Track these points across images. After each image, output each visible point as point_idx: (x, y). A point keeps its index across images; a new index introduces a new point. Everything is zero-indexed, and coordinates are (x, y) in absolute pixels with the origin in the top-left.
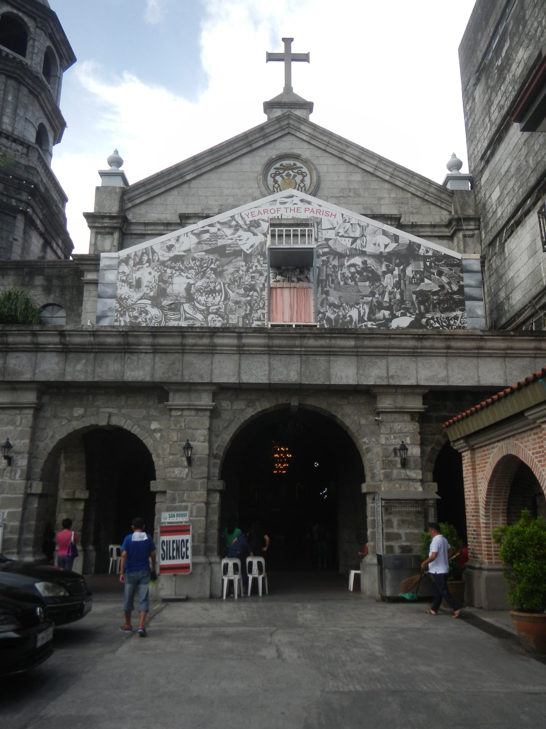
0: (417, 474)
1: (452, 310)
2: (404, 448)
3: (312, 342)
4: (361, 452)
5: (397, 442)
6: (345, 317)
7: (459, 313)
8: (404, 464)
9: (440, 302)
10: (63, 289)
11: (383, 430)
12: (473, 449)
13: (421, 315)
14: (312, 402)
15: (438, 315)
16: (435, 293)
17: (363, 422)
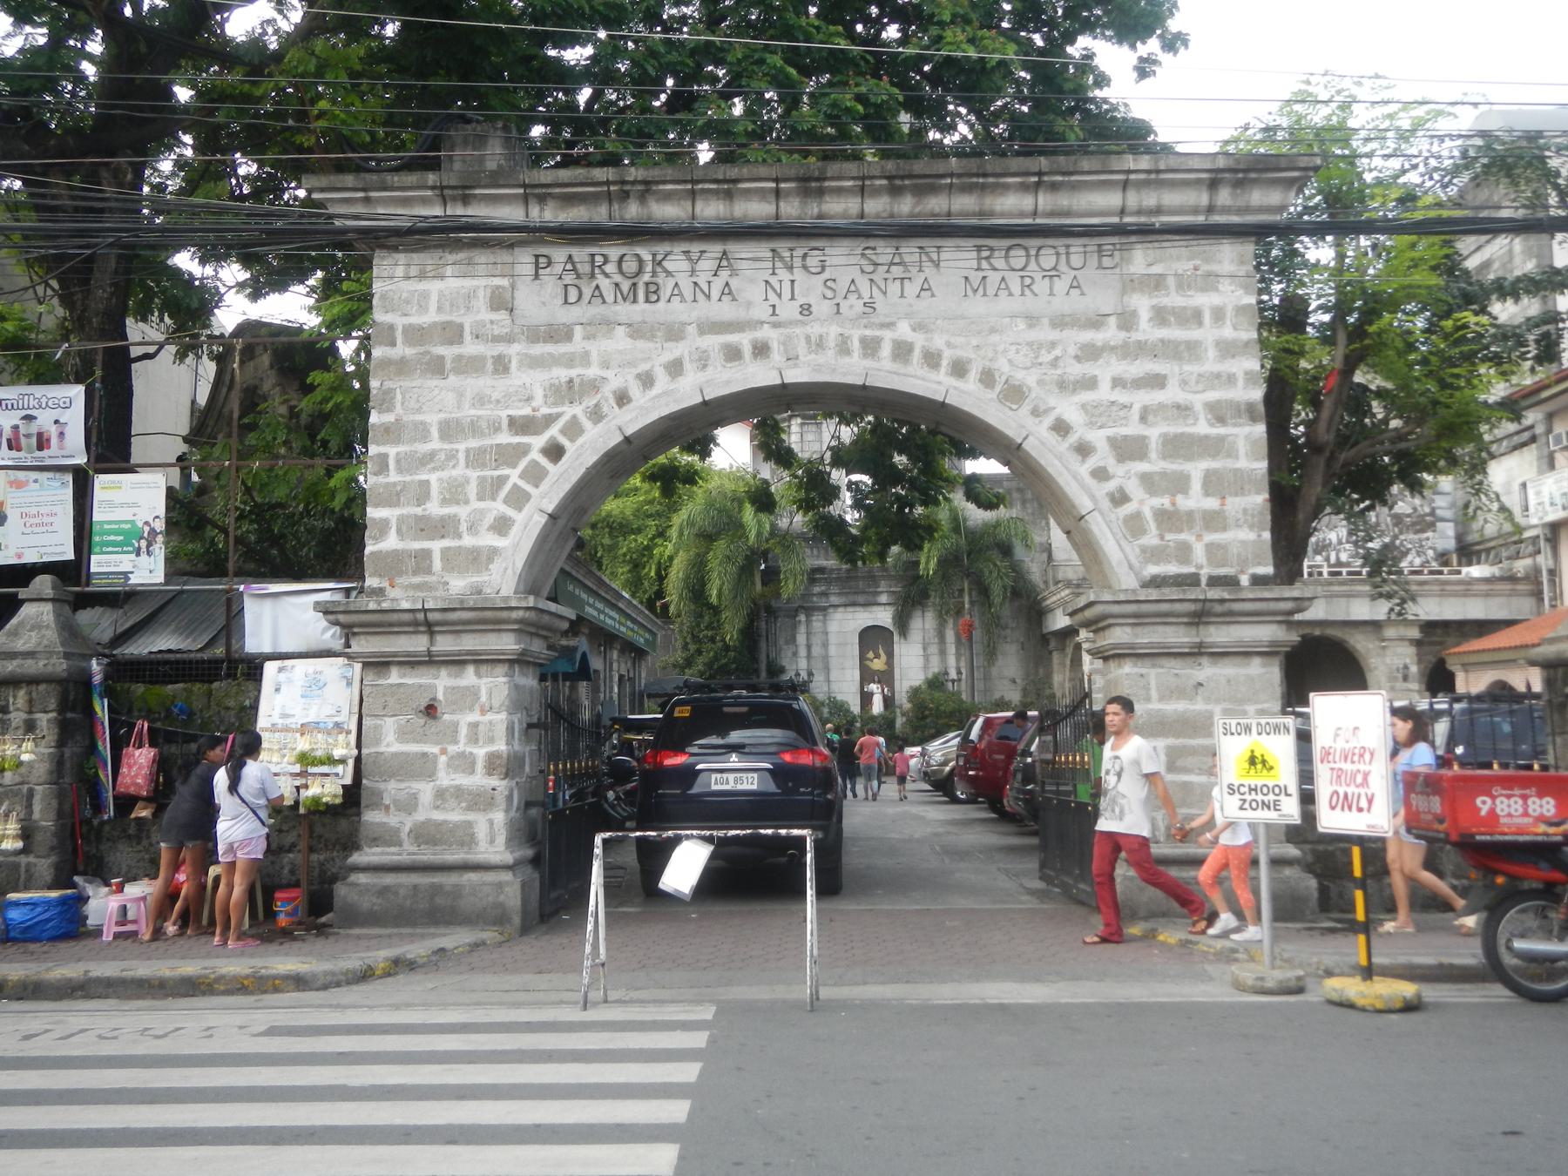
0: (1415, 686)
1: (1423, 531)
2: (1406, 667)
3: (1336, 588)
4: (1366, 670)
5: (1399, 663)
6: (1324, 540)
7: (1430, 534)
8: (1405, 679)
9: (1414, 524)
10: (1024, 502)
11: (1388, 652)
12: (1466, 671)
13: (1396, 537)
14: (1330, 632)
15: (1411, 536)
16: (1409, 516)
17: (1371, 646)
